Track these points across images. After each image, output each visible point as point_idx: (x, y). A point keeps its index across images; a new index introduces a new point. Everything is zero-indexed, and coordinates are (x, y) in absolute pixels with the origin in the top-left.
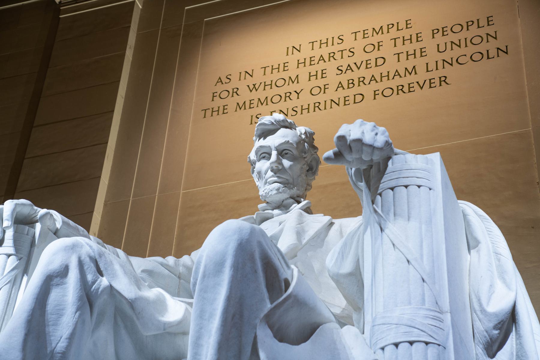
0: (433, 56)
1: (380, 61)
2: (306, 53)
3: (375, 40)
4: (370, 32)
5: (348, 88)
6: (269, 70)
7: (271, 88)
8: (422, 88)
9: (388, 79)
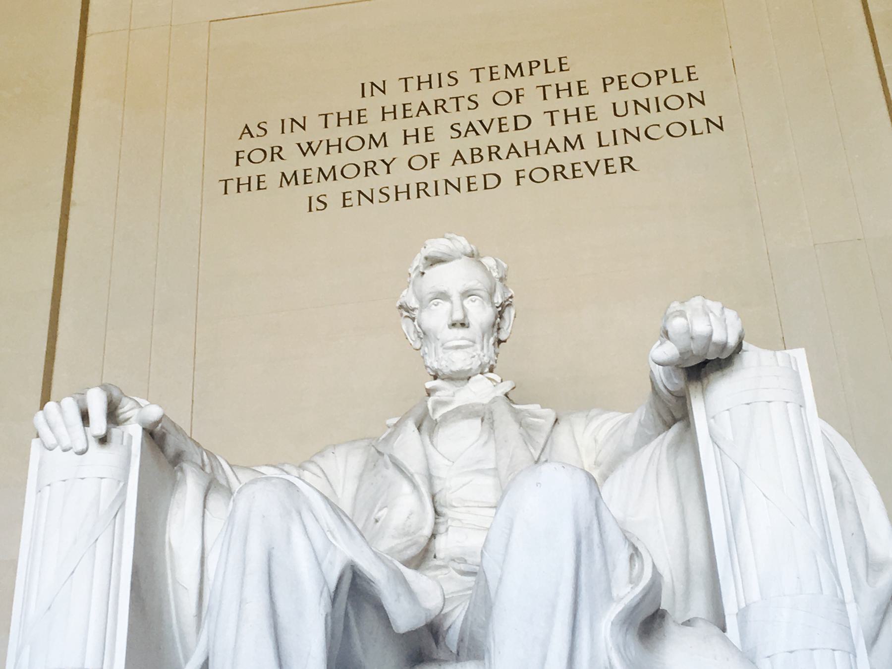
0: (606, 123)
2: (395, 96)
3: (512, 84)
4: (502, 71)
5: (473, 162)
6: (332, 120)
7: (340, 151)
8: (593, 173)
9: (538, 153)
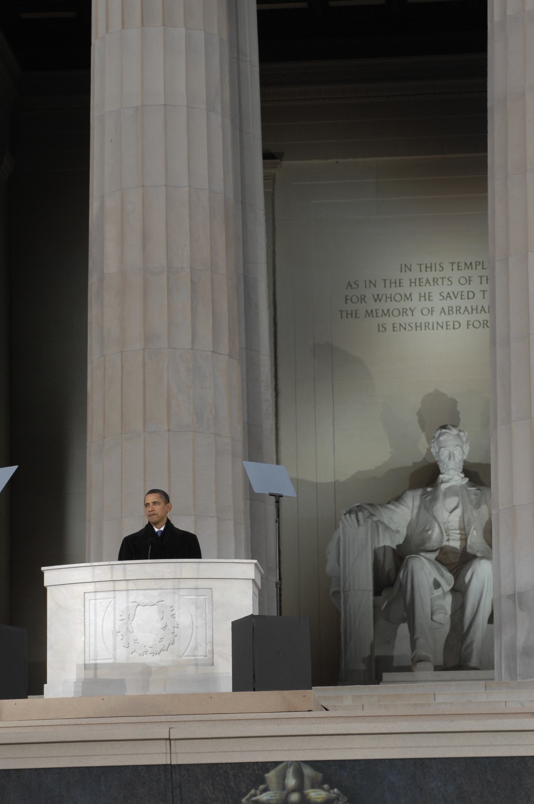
1: (471, 295)
5: (449, 314)
9: (477, 313)
